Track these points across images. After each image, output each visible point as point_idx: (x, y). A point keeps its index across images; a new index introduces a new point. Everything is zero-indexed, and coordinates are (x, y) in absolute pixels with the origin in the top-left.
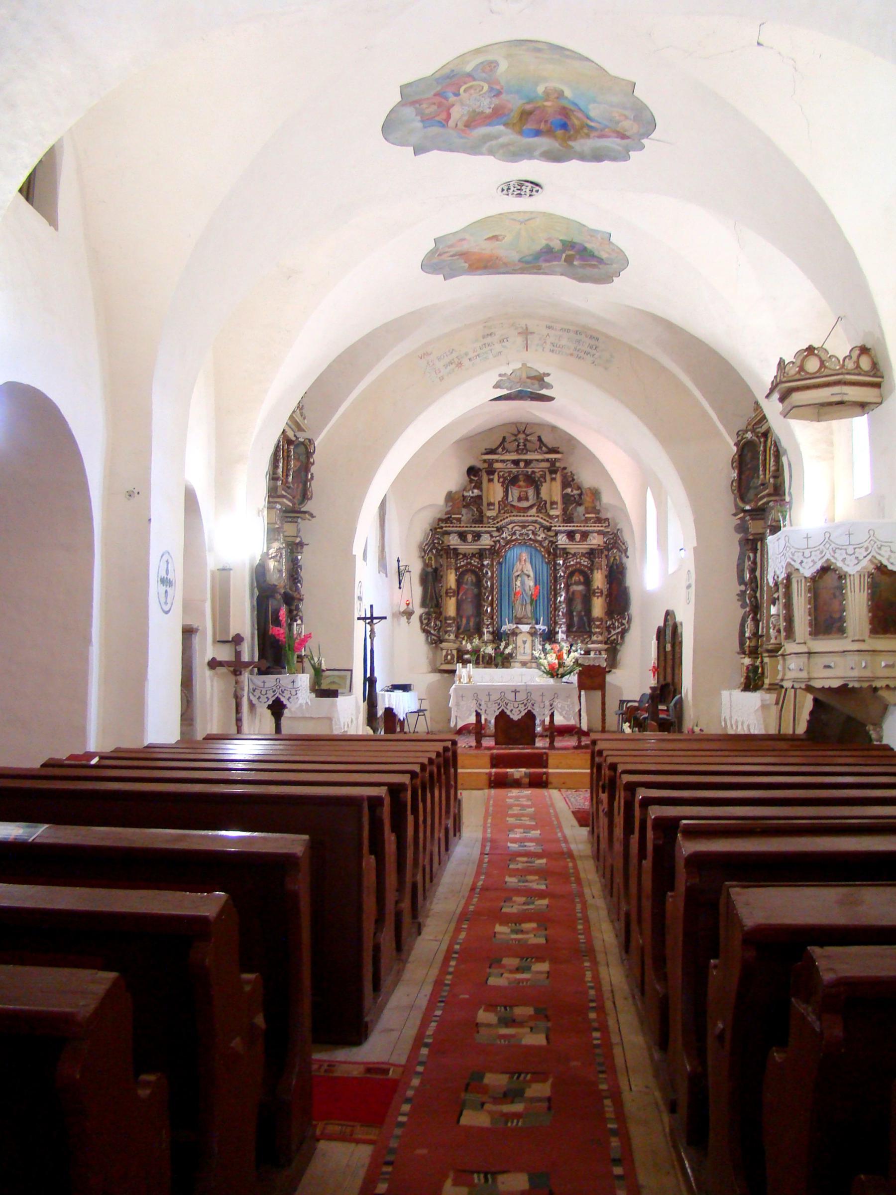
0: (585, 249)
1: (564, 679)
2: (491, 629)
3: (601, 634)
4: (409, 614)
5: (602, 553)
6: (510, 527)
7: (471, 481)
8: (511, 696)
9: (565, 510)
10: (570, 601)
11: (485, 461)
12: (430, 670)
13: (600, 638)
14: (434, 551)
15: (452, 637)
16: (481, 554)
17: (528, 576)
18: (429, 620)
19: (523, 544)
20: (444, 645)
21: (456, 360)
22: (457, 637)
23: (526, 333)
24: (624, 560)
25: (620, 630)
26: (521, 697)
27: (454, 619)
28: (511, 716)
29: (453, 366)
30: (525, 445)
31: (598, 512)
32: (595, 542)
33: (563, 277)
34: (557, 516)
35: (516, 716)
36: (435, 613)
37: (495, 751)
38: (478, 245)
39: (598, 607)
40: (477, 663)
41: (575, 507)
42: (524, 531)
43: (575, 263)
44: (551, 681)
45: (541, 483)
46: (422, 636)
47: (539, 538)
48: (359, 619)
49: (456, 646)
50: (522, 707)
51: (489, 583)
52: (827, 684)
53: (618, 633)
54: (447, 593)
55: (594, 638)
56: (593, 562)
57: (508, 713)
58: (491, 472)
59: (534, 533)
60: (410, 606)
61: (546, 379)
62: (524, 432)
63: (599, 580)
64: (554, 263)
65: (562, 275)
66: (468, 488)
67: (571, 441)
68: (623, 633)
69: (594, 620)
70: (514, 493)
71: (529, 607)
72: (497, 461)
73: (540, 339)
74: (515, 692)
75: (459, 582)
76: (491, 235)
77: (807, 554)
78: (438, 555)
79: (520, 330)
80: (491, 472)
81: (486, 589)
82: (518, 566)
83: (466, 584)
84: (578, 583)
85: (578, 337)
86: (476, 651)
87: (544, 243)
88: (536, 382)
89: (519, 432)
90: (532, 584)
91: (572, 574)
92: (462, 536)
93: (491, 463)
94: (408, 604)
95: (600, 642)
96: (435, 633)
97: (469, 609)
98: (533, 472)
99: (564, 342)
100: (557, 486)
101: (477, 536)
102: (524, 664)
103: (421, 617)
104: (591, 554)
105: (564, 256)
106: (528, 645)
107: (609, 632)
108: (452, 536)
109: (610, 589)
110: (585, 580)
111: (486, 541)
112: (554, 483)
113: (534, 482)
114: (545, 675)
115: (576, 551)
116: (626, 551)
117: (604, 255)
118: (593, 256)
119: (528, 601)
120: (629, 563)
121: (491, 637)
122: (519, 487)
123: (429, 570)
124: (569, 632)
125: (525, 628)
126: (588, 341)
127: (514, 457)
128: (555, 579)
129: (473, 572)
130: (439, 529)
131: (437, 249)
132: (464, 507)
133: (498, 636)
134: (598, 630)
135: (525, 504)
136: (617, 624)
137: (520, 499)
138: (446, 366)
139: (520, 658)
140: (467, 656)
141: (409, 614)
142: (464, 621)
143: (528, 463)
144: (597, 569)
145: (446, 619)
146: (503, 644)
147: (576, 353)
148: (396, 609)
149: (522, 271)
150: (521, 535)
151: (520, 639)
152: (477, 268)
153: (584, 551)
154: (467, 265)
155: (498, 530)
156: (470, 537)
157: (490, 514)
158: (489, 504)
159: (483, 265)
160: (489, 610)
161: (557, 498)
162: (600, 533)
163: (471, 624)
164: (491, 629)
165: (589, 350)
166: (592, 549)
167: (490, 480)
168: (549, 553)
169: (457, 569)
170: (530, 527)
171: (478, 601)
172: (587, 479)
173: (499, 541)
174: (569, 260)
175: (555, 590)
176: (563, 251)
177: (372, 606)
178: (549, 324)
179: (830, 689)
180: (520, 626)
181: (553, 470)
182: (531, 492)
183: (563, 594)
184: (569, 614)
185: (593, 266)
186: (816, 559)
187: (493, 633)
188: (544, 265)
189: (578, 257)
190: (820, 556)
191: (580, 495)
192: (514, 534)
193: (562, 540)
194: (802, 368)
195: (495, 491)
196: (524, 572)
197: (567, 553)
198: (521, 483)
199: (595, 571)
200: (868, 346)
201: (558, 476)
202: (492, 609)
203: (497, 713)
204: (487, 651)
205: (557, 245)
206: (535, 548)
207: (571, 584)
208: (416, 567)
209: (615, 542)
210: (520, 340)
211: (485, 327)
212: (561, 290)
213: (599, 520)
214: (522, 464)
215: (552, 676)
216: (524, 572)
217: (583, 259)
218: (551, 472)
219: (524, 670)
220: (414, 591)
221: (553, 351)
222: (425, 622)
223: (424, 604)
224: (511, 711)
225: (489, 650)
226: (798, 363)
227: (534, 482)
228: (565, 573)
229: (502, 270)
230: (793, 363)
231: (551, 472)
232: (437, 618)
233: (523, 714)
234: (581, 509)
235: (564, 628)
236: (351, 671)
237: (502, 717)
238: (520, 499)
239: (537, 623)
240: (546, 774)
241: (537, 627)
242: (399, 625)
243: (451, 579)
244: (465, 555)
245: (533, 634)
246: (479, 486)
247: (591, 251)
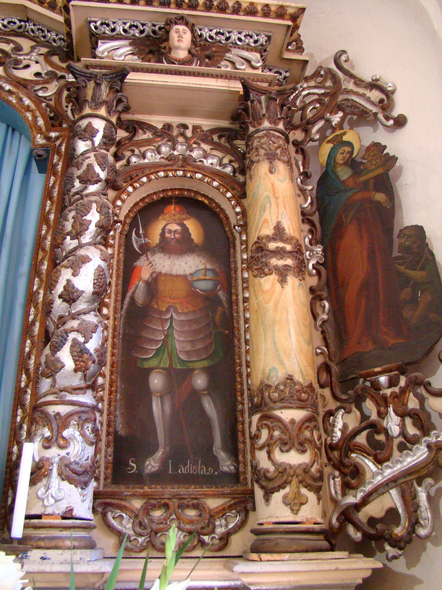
3: (316, 484)
25: (420, 454)
47: (27, 75)
53: (417, 474)
55: (274, 510)
63: (277, 200)
107: (352, 476)
110: (208, 235)
115: (175, 120)
134: (294, 458)
136: (393, 424)
144: (271, 157)
153: (207, 124)
199: (263, 168)
207: (146, 249)
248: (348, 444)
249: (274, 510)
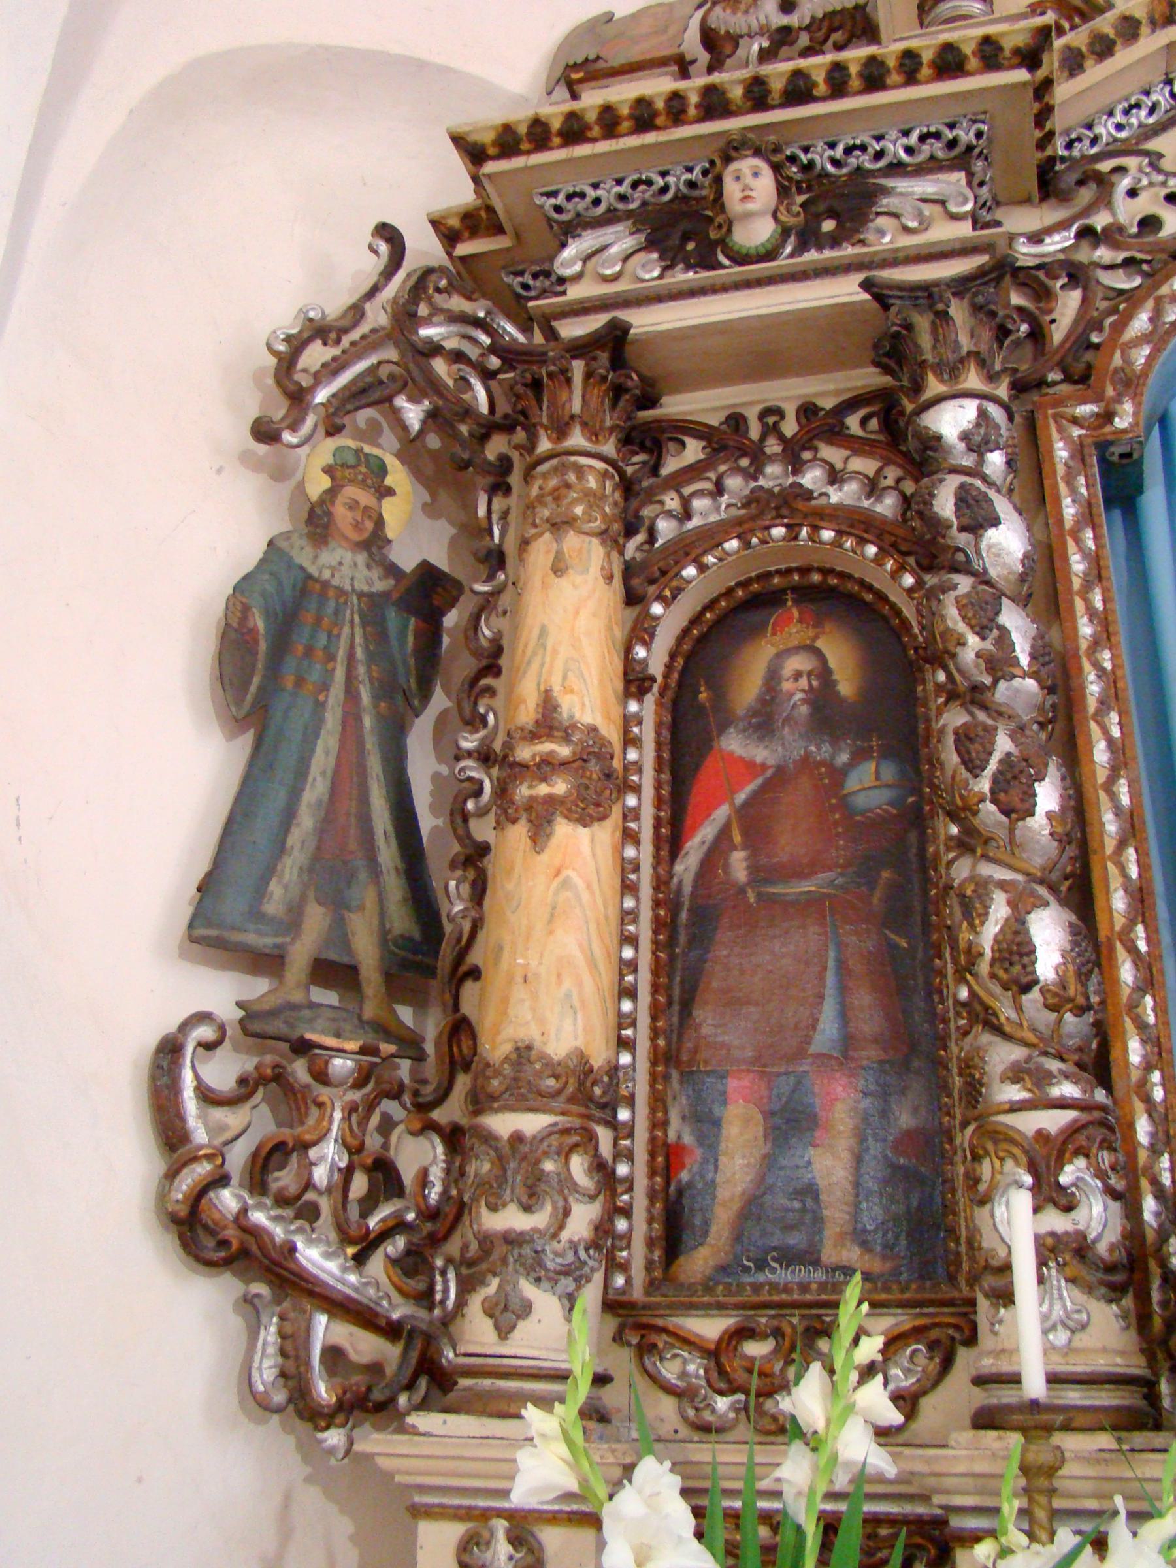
2: (1096, 1217)
14: (413, 414)
20: (436, 1442)
27: (589, 1094)
46: (193, 1322)
51: (1016, 623)
81: (976, 696)
83: (764, 721)
92: (686, 230)
96: (374, 1282)
121: (1105, 1336)
129: (833, 597)
160: (1049, 937)
164: (1096, 1217)
169: (638, 586)
171: (904, 892)
202: (1091, 945)
243: (570, 637)
244: (729, 440)
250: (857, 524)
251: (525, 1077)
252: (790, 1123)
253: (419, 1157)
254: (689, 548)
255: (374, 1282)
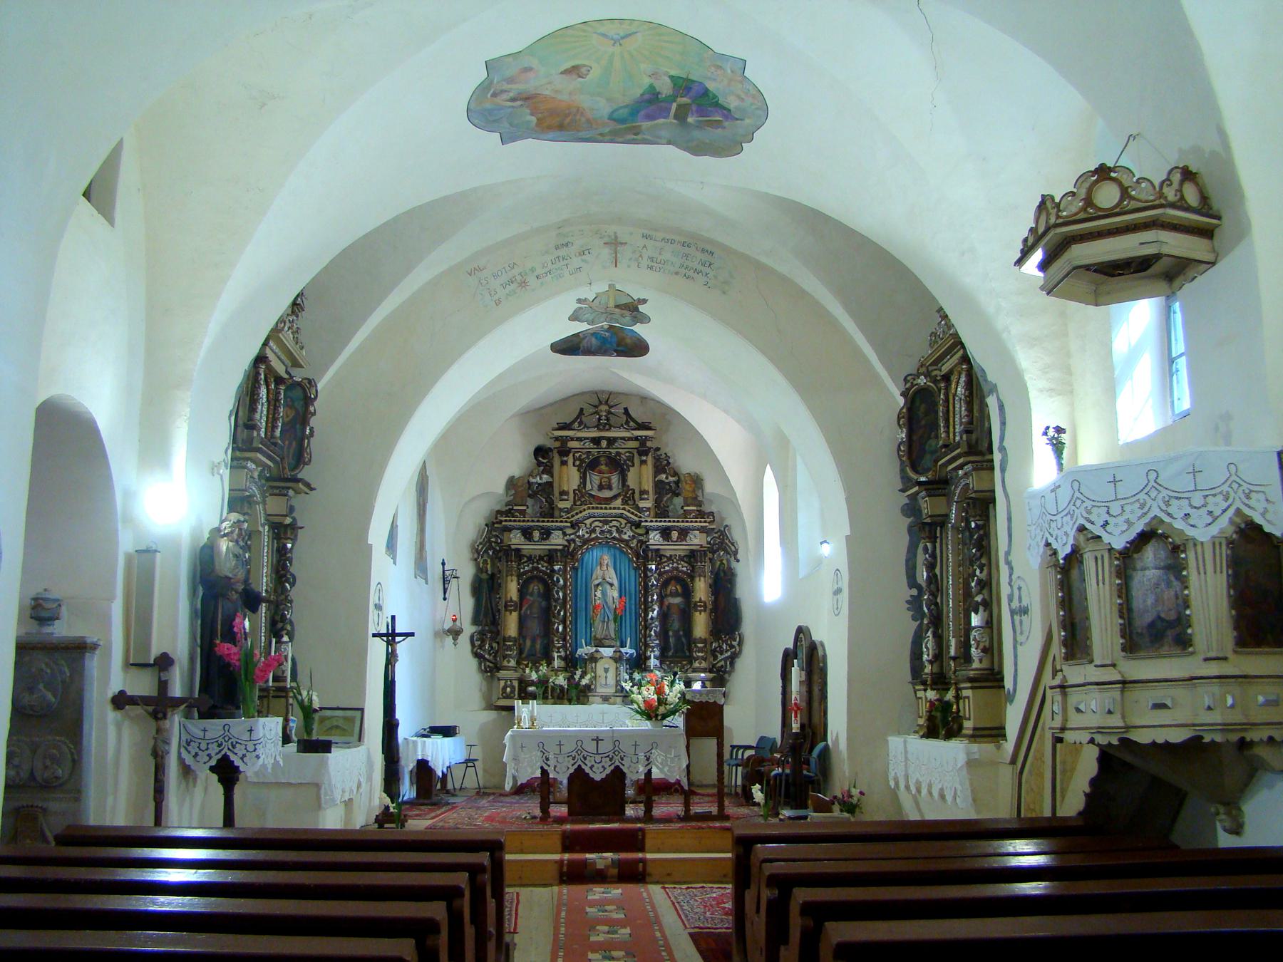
0: (706, 92)
1: (665, 722)
3: (705, 660)
4: (455, 633)
5: (705, 555)
6: (588, 522)
7: (539, 464)
8: (591, 747)
9: (658, 501)
10: (664, 616)
11: (557, 439)
12: (484, 705)
13: (704, 665)
15: (513, 663)
16: (551, 557)
17: (611, 585)
18: (483, 641)
19: (606, 543)
20: (502, 673)
21: (519, 278)
22: (518, 663)
23: (615, 244)
24: (734, 564)
26: (605, 747)
27: (515, 640)
28: (592, 775)
29: (513, 286)
30: (608, 419)
31: (700, 504)
32: (696, 541)
33: (671, 149)
34: (648, 509)
35: (598, 775)
36: (490, 632)
37: (568, 827)
38: (548, 81)
39: (701, 625)
40: (545, 698)
41: (671, 499)
42: (606, 527)
43: (690, 120)
44: (647, 725)
45: (628, 467)
46: (474, 662)
47: (626, 537)
48: (374, 635)
49: (517, 675)
50: (606, 762)
52: (1161, 737)
54: (506, 606)
55: (696, 665)
56: (693, 567)
57: (587, 770)
58: (564, 452)
59: (619, 531)
60: (458, 623)
61: (641, 308)
62: (606, 403)
63: (701, 589)
64: (661, 121)
65: (669, 143)
66: (535, 472)
67: (668, 415)
68: (733, 658)
69: (696, 641)
70: (594, 480)
71: (612, 625)
72: (572, 439)
73: (634, 252)
74: (597, 740)
75: (522, 592)
76: (568, 65)
77: (1115, 508)
78: (496, 557)
79: (606, 240)
80: (564, 452)
82: (598, 572)
83: (532, 594)
84: (675, 595)
85: (686, 250)
86: (543, 682)
87: (647, 81)
88: (627, 313)
89: (601, 403)
90: (616, 594)
91: (666, 584)
92: (527, 533)
93: (564, 440)
94: (454, 620)
95: (704, 670)
96: (491, 658)
97: (535, 627)
98: (618, 454)
99: (667, 255)
100: (648, 470)
101: (546, 533)
102: (606, 699)
103: (472, 637)
104: (692, 556)
105: (674, 105)
106: (611, 674)
107: (715, 657)
108: (515, 532)
109: (715, 603)
111: (557, 540)
112: (644, 467)
113: (619, 466)
114: (638, 716)
115: (672, 553)
116: (736, 553)
117: (732, 103)
118: (717, 106)
119: (611, 617)
120: (739, 568)
121: (562, 664)
122: (600, 472)
123: (484, 576)
124: (662, 658)
125: (607, 652)
126: (699, 255)
127: (594, 433)
128: (646, 588)
130: (497, 525)
131: (491, 83)
132: (529, 496)
133: (572, 663)
135: (607, 494)
137: (601, 487)
138: (504, 286)
139: (601, 690)
140: (531, 689)
141: (455, 633)
142: (528, 643)
143: (611, 441)
145: (505, 639)
146: (579, 673)
147: (683, 271)
148: (439, 627)
149: (613, 137)
150: (602, 532)
151: (600, 666)
152: (550, 128)
153: (683, 554)
154: (534, 119)
155: (573, 526)
156: (536, 534)
157: (562, 505)
158: (563, 493)
159: (558, 122)
160: (561, 628)
161: (648, 485)
162: (702, 530)
163: (538, 646)
164: (563, 654)
165: (700, 267)
166: (692, 551)
167: (564, 463)
168: (638, 556)
169: (519, 576)
170: (615, 523)
171: (547, 617)
172: (686, 462)
173: (574, 541)
174: (681, 116)
175: (646, 601)
176: (673, 98)
177: (393, 618)
178: (646, 232)
179: (1167, 744)
180: (601, 649)
181: (643, 451)
182: (615, 479)
183: (656, 608)
184: (663, 635)
185: (717, 124)
186: (1133, 518)
187: (565, 659)
188: (646, 124)
189: (694, 108)
190: (1140, 512)
191: (677, 483)
192: (593, 531)
193: (655, 539)
194: (1089, 202)
195: (570, 477)
196: (606, 579)
197: (661, 556)
198: (603, 467)
200: (1193, 169)
201: (650, 459)
202: (565, 628)
203: (572, 770)
204: (557, 682)
205: (665, 87)
206: (620, 549)
208: (467, 573)
209: (722, 542)
210: (606, 252)
211: (558, 235)
212: (668, 171)
213: (701, 514)
214: (604, 443)
215: (649, 718)
216: (606, 579)
217: (701, 112)
218: (641, 453)
219: (606, 706)
220: (462, 604)
221: (651, 268)
222: (478, 643)
223: (475, 621)
224: (591, 768)
225: (561, 680)
226: (1082, 193)
227: (619, 466)
228: (657, 580)
229: (582, 134)
230: (1073, 194)
231: (641, 453)
232: (492, 639)
233: (608, 771)
234: (678, 501)
235: (657, 653)
236: (362, 710)
237: (579, 777)
238: (601, 487)
239: (623, 645)
240: (643, 861)
241: (623, 650)
242: (443, 647)
243: (512, 589)
244: (530, 558)
245: (617, 659)
246: (548, 470)
247: (715, 96)
248: (715, 650)
249: (696, 665)
250: (545, 573)
251: (510, 639)
252: (534, 641)
253: (495, 645)
254: (525, 573)
255: (491, 658)
